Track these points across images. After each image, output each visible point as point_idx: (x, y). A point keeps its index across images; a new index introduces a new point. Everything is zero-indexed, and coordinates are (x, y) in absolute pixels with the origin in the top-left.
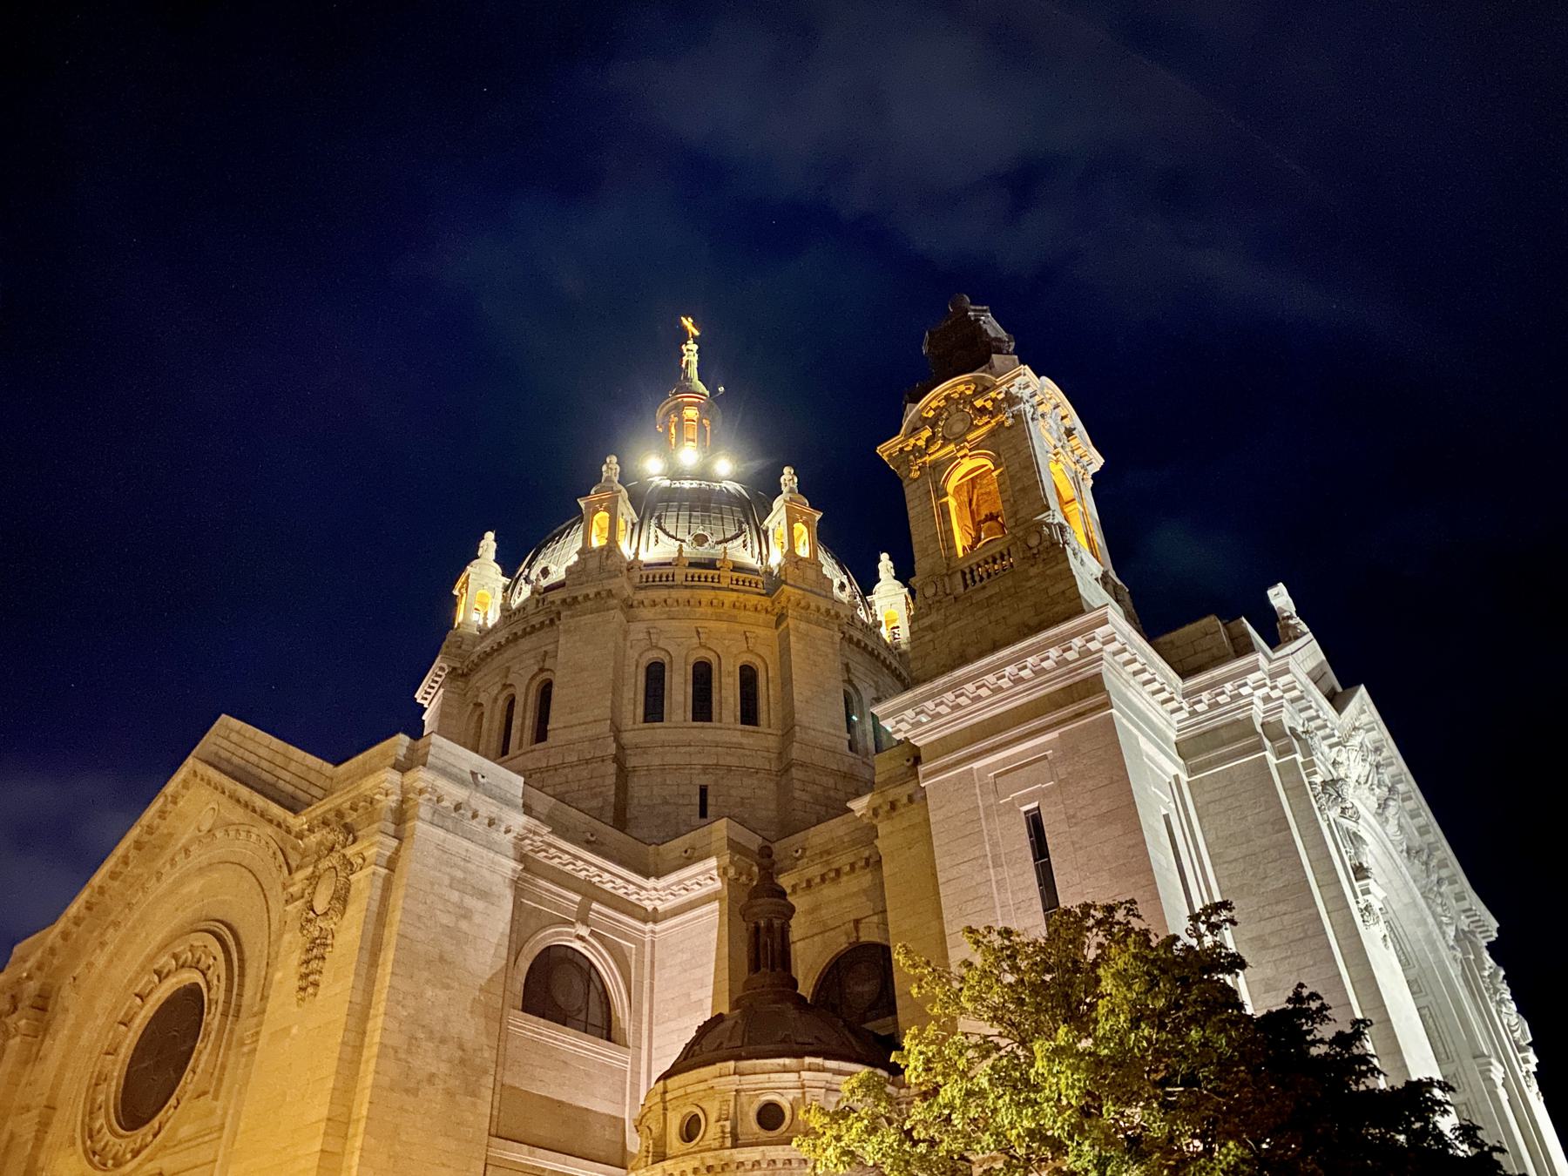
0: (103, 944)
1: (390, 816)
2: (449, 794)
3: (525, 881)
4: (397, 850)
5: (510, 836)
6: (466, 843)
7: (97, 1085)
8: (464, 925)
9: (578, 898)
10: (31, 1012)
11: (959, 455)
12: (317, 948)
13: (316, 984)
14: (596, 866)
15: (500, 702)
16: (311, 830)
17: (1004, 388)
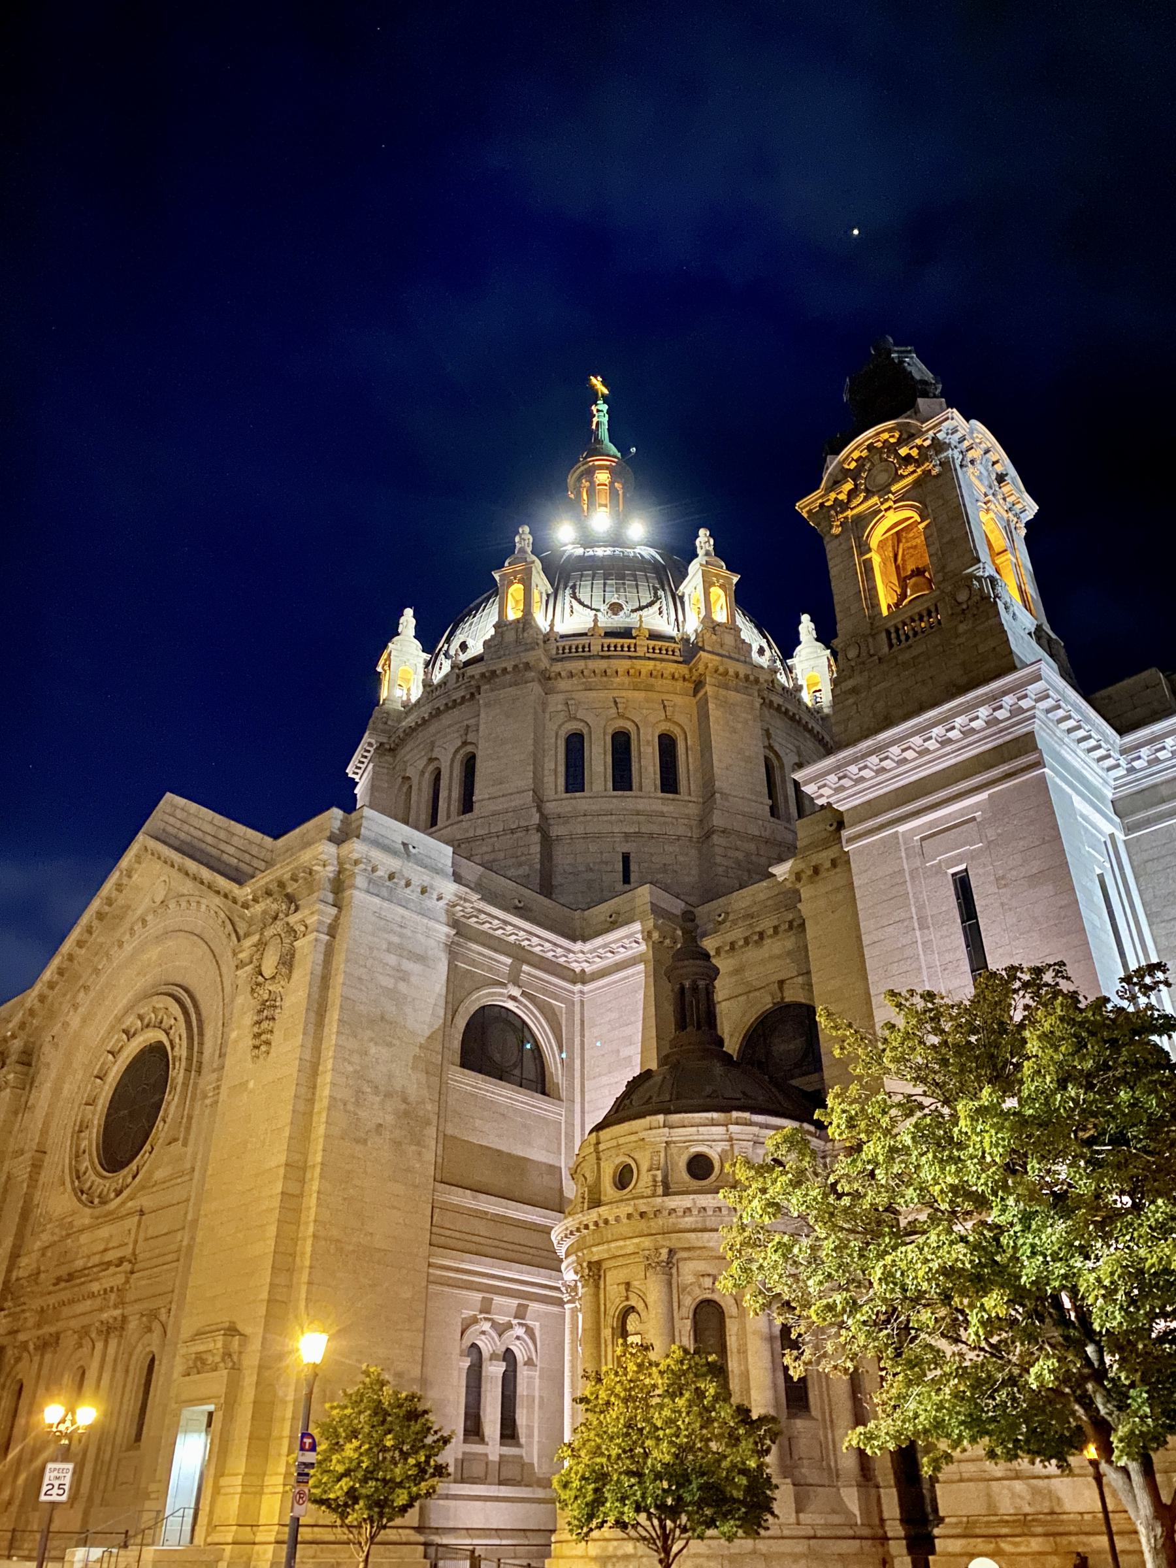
0: (75, 1007)
1: (328, 886)
2: (383, 864)
3: (458, 945)
4: (337, 918)
5: (442, 903)
6: (401, 910)
7: (81, 1131)
8: (402, 987)
9: (509, 961)
10: (19, 1068)
11: (883, 508)
12: (267, 1010)
13: (268, 1043)
14: (524, 930)
15: (427, 775)
16: (255, 900)
17: (931, 433)
